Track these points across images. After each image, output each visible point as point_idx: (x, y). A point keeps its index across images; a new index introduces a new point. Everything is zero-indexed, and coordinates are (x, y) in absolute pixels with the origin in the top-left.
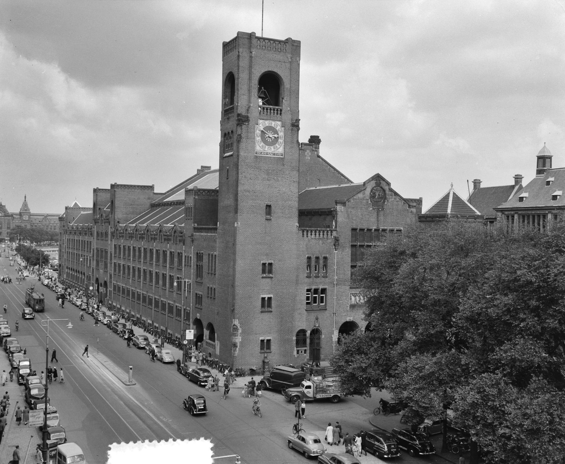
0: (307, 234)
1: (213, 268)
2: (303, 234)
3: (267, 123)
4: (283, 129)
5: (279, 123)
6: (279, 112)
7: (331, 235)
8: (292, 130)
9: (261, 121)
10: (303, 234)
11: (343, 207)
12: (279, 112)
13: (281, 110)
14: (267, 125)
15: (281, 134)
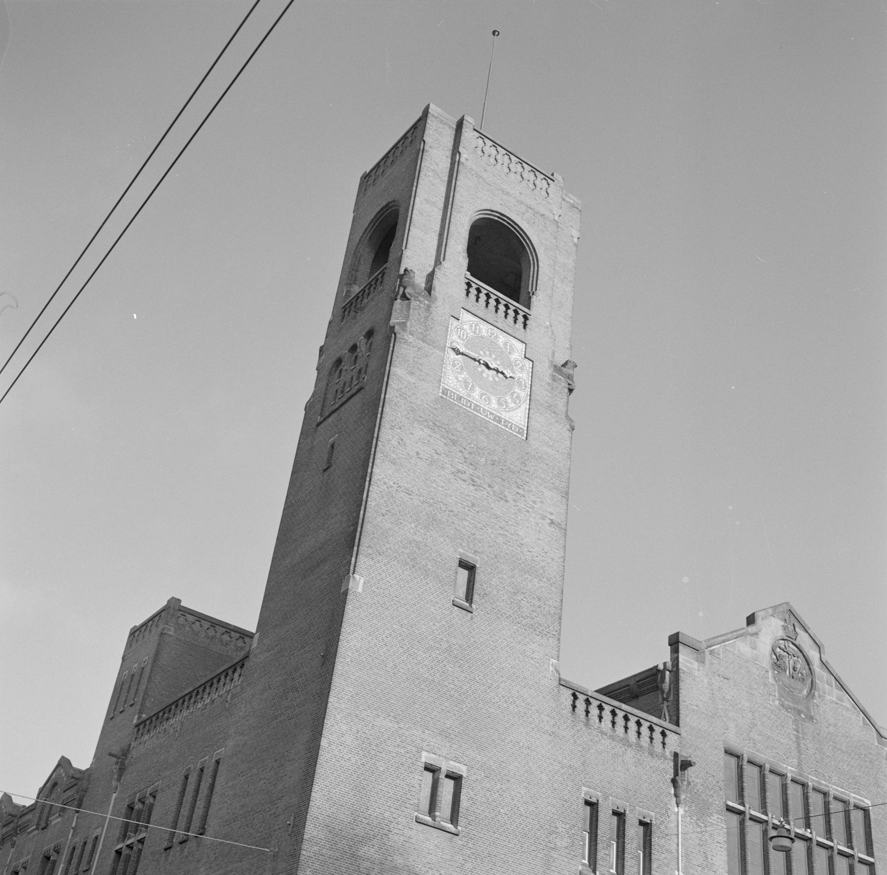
0: (587, 712)
1: (199, 812)
2: (574, 707)
3: (484, 328)
4: (528, 364)
5: (520, 346)
6: (520, 319)
7: (664, 744)
8: (554, 379)
9: (466, 317)
10: (574, 707)
11: (696, 664)
12: (520, 319)
13: (526, 318)
14: (484, 333)
15: (524, 376)
